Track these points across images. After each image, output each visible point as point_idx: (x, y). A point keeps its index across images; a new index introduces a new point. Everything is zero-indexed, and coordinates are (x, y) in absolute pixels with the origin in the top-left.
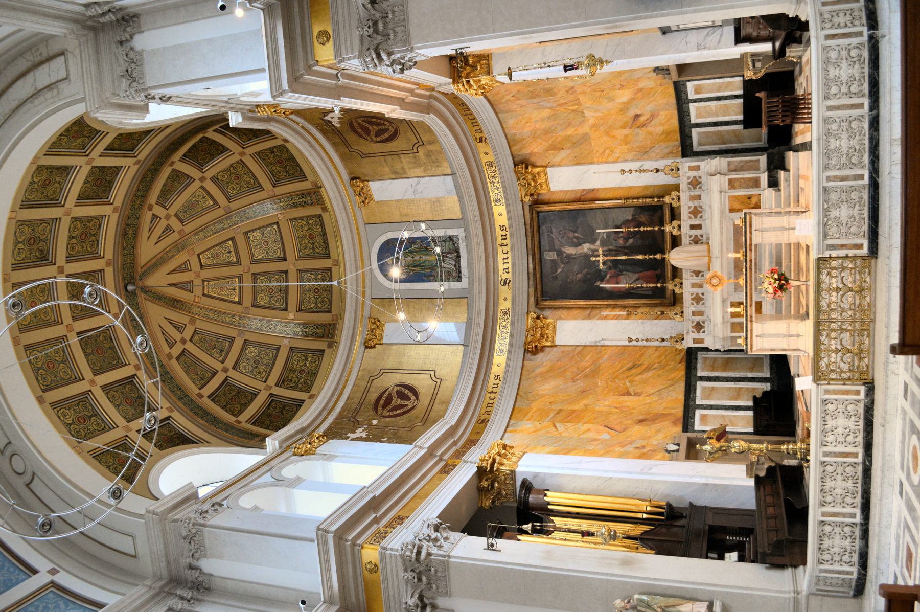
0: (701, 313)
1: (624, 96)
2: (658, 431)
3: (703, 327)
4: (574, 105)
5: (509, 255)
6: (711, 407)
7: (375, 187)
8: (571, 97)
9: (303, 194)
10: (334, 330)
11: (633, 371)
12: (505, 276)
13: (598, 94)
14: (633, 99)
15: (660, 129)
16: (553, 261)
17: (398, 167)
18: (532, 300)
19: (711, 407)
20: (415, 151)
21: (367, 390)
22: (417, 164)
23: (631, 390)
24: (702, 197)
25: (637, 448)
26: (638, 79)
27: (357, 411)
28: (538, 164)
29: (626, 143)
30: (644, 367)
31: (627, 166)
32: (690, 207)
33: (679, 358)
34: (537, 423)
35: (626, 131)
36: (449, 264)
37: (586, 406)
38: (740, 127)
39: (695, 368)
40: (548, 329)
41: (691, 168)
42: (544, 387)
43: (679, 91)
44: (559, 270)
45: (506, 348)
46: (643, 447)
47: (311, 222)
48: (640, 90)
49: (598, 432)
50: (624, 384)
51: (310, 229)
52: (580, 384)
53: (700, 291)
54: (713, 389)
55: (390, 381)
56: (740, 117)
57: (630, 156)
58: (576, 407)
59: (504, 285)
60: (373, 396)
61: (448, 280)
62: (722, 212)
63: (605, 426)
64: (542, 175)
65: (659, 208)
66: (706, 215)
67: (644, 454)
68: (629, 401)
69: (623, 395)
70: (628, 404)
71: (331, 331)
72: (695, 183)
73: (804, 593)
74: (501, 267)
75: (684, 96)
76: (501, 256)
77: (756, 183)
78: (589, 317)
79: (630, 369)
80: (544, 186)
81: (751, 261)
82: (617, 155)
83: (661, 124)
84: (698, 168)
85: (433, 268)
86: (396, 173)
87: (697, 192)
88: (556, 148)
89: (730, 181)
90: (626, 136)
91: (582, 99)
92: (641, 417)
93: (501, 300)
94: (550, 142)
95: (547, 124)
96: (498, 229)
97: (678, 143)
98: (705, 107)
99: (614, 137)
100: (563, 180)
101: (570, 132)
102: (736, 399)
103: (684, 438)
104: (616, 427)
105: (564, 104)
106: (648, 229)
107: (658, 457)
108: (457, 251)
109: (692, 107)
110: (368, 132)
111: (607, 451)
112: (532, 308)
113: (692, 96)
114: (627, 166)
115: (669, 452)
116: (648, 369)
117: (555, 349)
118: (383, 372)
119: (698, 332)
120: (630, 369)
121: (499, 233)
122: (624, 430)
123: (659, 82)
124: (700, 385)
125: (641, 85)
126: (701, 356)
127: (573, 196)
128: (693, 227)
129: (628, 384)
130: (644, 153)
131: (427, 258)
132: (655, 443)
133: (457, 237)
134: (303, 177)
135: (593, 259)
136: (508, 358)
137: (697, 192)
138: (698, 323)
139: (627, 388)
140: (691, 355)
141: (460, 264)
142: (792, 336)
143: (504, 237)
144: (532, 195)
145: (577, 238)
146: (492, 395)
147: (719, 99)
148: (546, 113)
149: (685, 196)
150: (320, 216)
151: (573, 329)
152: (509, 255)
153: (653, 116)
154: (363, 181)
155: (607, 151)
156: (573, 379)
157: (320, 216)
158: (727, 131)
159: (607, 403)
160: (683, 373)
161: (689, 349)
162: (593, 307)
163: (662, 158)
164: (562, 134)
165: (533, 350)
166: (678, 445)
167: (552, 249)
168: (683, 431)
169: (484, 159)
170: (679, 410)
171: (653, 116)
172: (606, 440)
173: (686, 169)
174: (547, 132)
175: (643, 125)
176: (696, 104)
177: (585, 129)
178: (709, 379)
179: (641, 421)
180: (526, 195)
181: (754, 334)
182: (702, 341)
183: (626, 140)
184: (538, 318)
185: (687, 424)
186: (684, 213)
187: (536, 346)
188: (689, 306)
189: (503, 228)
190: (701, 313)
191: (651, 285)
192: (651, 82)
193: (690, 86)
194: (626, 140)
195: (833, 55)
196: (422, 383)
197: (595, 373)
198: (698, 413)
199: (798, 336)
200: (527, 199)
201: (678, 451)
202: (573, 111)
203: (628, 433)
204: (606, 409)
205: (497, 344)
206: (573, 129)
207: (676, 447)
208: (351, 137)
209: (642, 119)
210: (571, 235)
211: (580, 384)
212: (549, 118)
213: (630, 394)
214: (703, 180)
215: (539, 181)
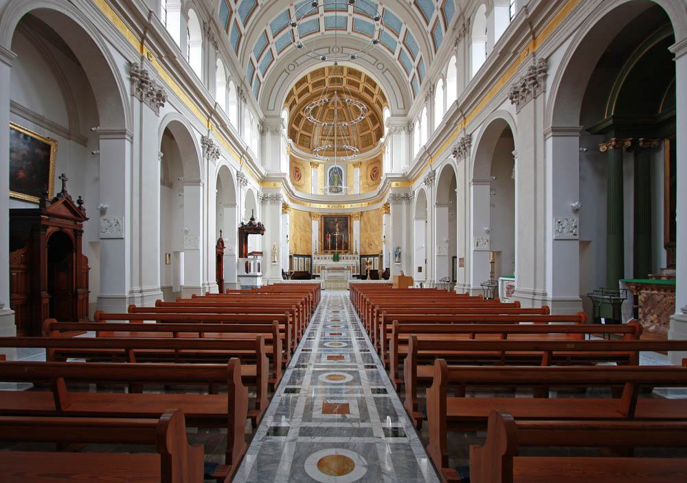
1: (376, 242)
21: (299, 164)
22: (363, 184)
27: (296, 162)
36: (334, 190)
43: (377, 255)
52: (302, 227)
55: (302, 171)
72: (354, 258)
77: (354, 272)
100: (356, 225)
103: (292, 255)
110: (374, 171)
116: (307, 245)
118: (304, 168)
140: (310, 256)
151: (316, 225)
153: (371, 249)
165: (310, 214)
169: (363, 204)
170: (297, 253)
171: (371, 249)
174: (369, 222)
183: (365, 242)
185: (295, 255)
192: (379, 249)
193: (377, 258)
194: (365, 242)
196: (302, 181)
208: (373, 166)
213: (301, 240)
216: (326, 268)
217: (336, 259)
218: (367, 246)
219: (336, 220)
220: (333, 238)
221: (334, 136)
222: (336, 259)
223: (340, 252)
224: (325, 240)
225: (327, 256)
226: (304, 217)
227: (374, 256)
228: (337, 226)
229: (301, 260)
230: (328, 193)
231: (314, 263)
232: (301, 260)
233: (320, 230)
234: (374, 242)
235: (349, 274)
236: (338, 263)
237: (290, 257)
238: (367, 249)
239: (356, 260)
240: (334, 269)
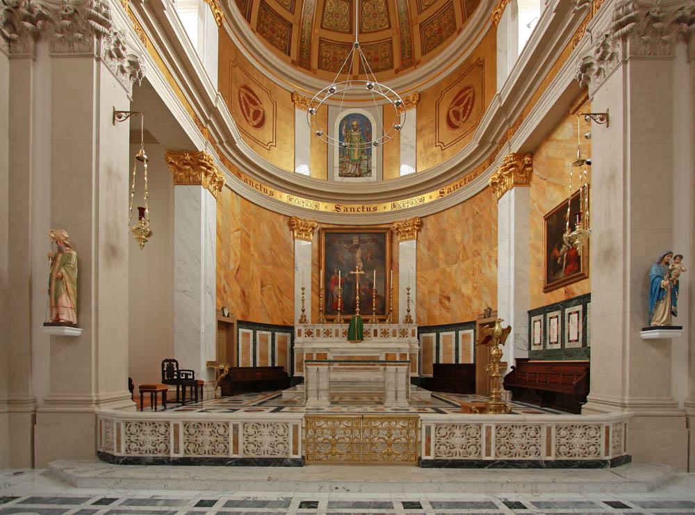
0: (318, 334)
1: (467, 290)
2: (237, 303)
3: (309, 336)
4: (463, 257)
5: (356, 212)
6: (255, 340)
7: (412, 113)
8: (470, 254)
9: (411, 53)
10: (305, 68)
11: (277, 291)
12: (342, 209)
13: (471, 273)
14: (463, 296)
15: (437, 313)
16: (352, 242)
17: (426, 132)
18: (325, 226)
19: (255, 340)
20: (437, 144)
23: (264, 288)
24: (394, 338)
25: (224, 287)
26: (480, 298)
28: (419, 233)
29: (429, 292)
30: (280, 298)
31: (413, 292)
32: (388, 330)
33: (286, 321)
34: (239, 217)
35: (438, 292)
36: (351, 168)
37: (253, 255)
38: (434, 361)
39: (280, 331)
40: (306, 235)
41: (413, 331)
42: (265, 226)
44: (345, 246)
45: (292, 203)
46: (225, 292)
47: (388, 60)
48: (470, 300)
49: (235, 261)
50: (269, 284)
51: (383, 59)
52: (268, 254)
53: (333, 334)
54: (267, 342)
56: (441, 362)
57: (419, 295)
58: (252, 248)
59: (336, 207)
60: (257, 90)
61: (340, 167)
62: (386, 349)
63: (239, 267)
64: (411, 237)
65: (384, 313)
66: (383, 340)
67: (220, 292)
68: (257, 286)
69: (262, 283)
70: (255, 285)
71: (304, 65)
73: (97, 409)
74: (348, 206)
75: (460, 328)
76: (356, 206)
78: (313, 264)
79: (279, 288)
80: (404, 238)
81: (374, 365)
82: (421, 286)
83: (440, 315)
84: (413, 335)
85: (349, 156)
86: (421, 130)
87: (398, 334)
88: (430, 247)
89: (406, 354)
90: (434, 292)
91: (468, 262)
92: (246, 293)
93: (325, 204)
94: (435, 242)
95: (449, 238)
96: (375, 205)
97: (426, 325)
98: (451, 341)
99: (434, 285)
100: (406, 252)
101: (441, 255)
102: (261, 356)
104: (238, 275)
105: (465, 250)
106: (374, 304)
107: (219, 302)
108: (360, 176)
109: (453, 333)
111: (221, 265)
112: (320, 226)
113: (461, 333)
114: (413, 292)
115: (223, 309)
116: (280, 301)
117: (292, 239)
119: (305, 333)
120: (279, 288)
121: (372, 206)
122: (237, 280)
123: (476, 312)
124: (269, 333)
125: (475, 300)
126: (289, 335)
127: (394, 258)
128: (375, 331)
129: (269, 286)
130: (420, 303)
131: (356, 153)
132: (229, 301)
133: (370, 176)
134: (424, 53)
135: (357, 267)
136: (284, 203)
137: (398, 334)
138: (312, 333)
139: (265, 286)
140: (289, 329)
141: (351, 176)
142: (318, 393)
143: (368, 209)
144: (397, 229)
145: (367, 258)
146: (259, 187)
147: (457, 349)
148: (459, 238)
149: (394, 326)
150: (392, 68)
151: (305, 248)
152: (356, 212)
153: (448, 309)
154: (417, 104)
155: (424, 280)
156: (272, 249)
157: (392, 68)
158: (432, 354)
159: (256, 270)
160: (277, 323)
161: (293, 328)
162: (320, 268)
163: (416, 315)
164: (441, 250)
166: (228, 316)
167: (361, 241)
168: (238, 321)
171: (448, 309)
172: (229, 266)
173: (413, 328)
174: (443, 240)
175: (441, 303)
176: (454, 335)
177: (442, 265)
178: (273, 340)
179: (244, 293)
180: (398, 225)
181: (319, 367)
182: (300, 335)
183: (431, 292)
184: (313, 228)
185: (243, 324)
186: (385, 326)
187: (294, 225)
188: (322, 327)
189: (375, 209)
190: (318, 334)
191: (339, 304)
192: (478, 306)
193: (472, 331)
195: (592, 433)
197: (275, 264)
198: (251, 331)
199: (318, 397)
200: (395, 225)
201: (224, 315)
202: (458, 257)
203: (235, 283)
204: (251, 268)
205: (295, 197)
206: (443, 257)
207: (226, 315)
209: (446, 302)
210: (369, 255)
211: (268, 254)
212: (454, 240)
213: (262, 286)
214: (405, 339)
215: (407, 235)
216: (330, 357)
217: (355, 334)
218: (435, 302)
219: (356, 240)
220: (349, 284)
221: (351, 32)
222: (355, 334)
223: (366, 321)
224: (328, 292)
225: (333, 327)
226: (273, 229)
227: (457, 327)
228: (358, 254)
229: (264, 339)
230: (338, 179)
231: (296, 346)
232: (264, 339)
233: (317, 265)
234: (455, 290)
235: (399, 377)
236: (360, 345)
237: (224, 326)
238: (437, 312)
239: (410, 338)
240: (349, 362)
